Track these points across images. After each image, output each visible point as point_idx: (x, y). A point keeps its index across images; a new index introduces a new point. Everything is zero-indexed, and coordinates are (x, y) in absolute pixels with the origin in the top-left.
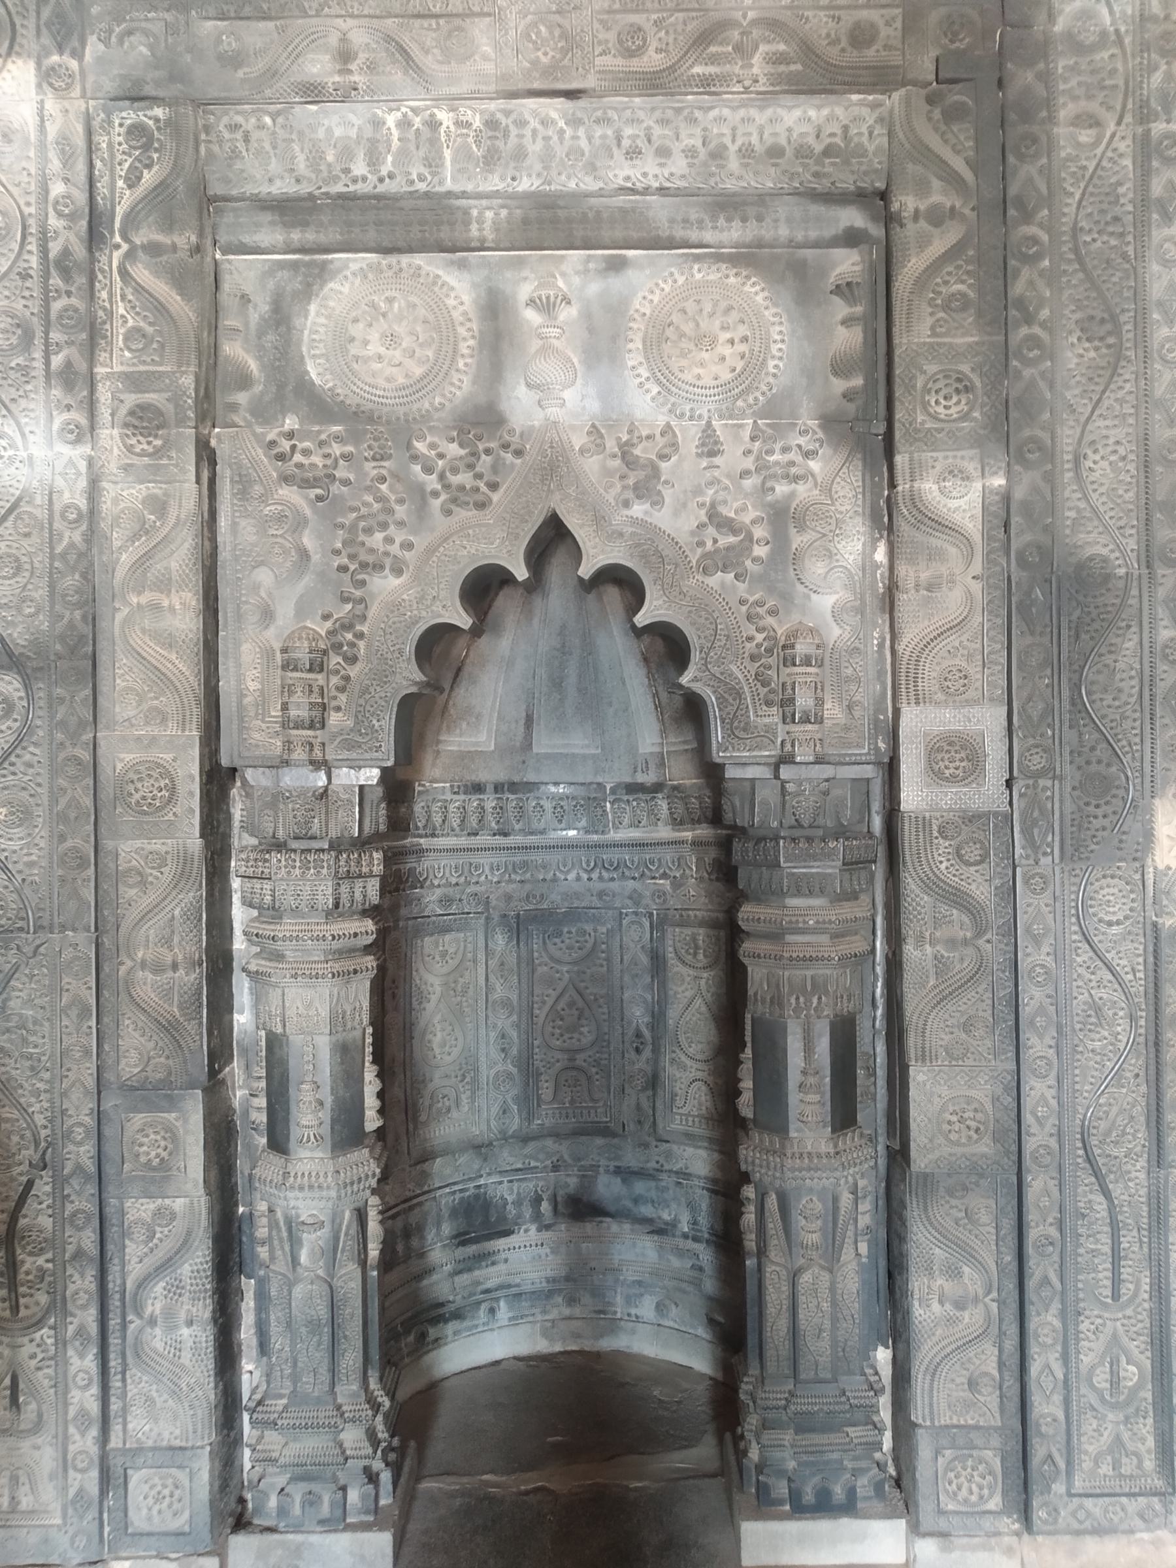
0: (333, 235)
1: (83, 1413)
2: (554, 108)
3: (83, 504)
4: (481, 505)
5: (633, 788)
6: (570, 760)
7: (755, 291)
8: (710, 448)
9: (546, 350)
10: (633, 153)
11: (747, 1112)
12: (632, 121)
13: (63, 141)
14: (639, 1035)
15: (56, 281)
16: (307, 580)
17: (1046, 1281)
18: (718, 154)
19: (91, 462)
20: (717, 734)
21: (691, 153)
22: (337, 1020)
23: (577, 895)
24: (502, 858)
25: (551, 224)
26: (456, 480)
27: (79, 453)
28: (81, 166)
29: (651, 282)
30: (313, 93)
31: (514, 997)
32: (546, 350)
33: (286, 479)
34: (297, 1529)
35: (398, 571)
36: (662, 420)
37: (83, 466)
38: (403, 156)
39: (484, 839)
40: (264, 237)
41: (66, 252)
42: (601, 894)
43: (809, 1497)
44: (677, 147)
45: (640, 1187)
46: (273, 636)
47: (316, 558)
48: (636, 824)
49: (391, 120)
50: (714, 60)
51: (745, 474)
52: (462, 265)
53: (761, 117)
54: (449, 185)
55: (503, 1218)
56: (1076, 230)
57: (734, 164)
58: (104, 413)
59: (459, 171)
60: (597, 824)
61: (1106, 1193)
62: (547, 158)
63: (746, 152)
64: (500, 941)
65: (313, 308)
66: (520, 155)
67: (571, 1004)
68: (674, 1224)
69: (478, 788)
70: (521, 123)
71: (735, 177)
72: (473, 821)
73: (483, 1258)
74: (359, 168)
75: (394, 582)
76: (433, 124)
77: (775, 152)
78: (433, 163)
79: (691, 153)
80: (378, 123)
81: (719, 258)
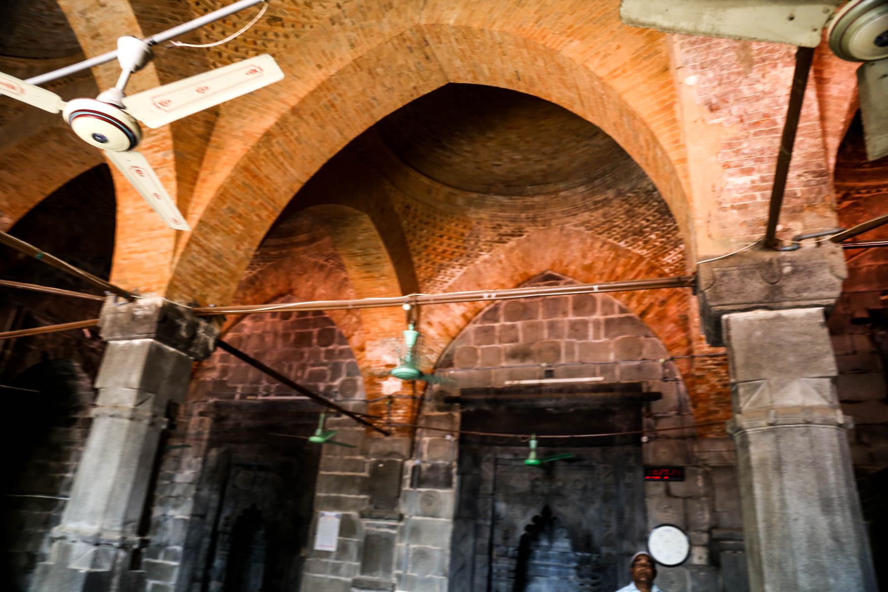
25: (261, 468)
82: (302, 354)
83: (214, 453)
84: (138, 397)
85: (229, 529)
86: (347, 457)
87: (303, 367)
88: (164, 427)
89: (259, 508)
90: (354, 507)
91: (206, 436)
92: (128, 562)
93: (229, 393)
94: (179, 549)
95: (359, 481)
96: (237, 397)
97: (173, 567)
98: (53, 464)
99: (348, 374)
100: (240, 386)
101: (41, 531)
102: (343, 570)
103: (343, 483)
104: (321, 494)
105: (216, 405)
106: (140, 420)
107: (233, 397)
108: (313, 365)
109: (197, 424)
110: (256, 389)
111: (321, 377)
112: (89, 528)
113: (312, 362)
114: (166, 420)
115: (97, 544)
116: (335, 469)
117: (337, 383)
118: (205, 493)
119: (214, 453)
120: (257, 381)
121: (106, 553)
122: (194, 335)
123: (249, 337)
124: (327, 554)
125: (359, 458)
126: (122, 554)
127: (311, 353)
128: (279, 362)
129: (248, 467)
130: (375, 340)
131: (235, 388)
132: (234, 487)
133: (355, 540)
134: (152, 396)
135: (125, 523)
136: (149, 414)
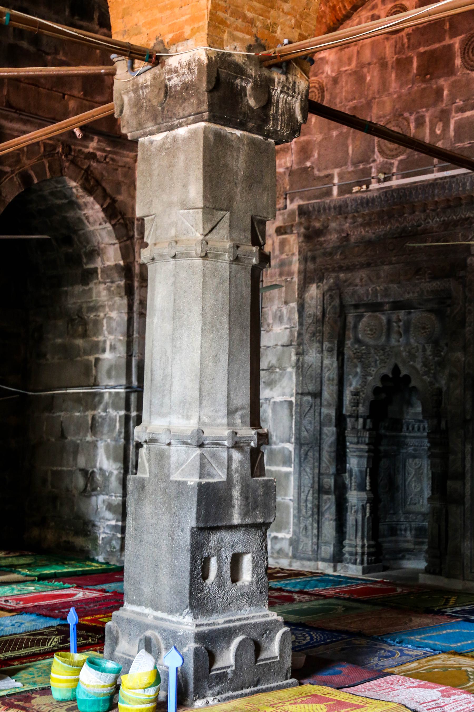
4: (385, 363)
7: (433, 317)
8: (424, 350)
10: (409, 293)
16: (358, 378)
21: (418, 292)
25: (397, 306)
29: (416, 315)
33: (355, 358)
34: (348, 563)
36: (416, 344)
46: (352, 388)
49: (370, 289)
52: (384, 314)
53: (430, 284)
54: (379, 300)
57: (425, 294)
58: (324, 349)
59: (381, 299)
63: (427, 291)
65: (361, 324)
74: (365, 299)
78: (377, 297)
79: (418, 292)
80: (368, 290)
83: (313, 291)
84: (205, 221)
85: (362, 409)
87: (444, 116)
88: (254, 261)
89: (404, 372)
91: (295, 267)
92: (248, 466)
93: (321, 186)
94: (290, 447)
96: (335, 191)
97: (287, 475)
98: (79, 342)
100: (336, 171)
101: (89, 438)
105: (302, 211)
106: (217, 256)
107: (329, 193)
108: (462, 110)
109: (286, 250)
110: (367, 172)
112: (187, 424)
113: (459, 103)
114: (254, 249)
115: (201, 445)
118: (312, 357)
119: (313, 291)
120: (366, 158)
121: (214, 455)
122: (268, 103)
123: (335, 81)
126: (236, 456)
127: (453, 85)
128: (398, 115)
129: (375, 307)
131: (330, 177)
132: (357, 341)
134: (228, 214)
135: (231, 413)
136: (228, 244)
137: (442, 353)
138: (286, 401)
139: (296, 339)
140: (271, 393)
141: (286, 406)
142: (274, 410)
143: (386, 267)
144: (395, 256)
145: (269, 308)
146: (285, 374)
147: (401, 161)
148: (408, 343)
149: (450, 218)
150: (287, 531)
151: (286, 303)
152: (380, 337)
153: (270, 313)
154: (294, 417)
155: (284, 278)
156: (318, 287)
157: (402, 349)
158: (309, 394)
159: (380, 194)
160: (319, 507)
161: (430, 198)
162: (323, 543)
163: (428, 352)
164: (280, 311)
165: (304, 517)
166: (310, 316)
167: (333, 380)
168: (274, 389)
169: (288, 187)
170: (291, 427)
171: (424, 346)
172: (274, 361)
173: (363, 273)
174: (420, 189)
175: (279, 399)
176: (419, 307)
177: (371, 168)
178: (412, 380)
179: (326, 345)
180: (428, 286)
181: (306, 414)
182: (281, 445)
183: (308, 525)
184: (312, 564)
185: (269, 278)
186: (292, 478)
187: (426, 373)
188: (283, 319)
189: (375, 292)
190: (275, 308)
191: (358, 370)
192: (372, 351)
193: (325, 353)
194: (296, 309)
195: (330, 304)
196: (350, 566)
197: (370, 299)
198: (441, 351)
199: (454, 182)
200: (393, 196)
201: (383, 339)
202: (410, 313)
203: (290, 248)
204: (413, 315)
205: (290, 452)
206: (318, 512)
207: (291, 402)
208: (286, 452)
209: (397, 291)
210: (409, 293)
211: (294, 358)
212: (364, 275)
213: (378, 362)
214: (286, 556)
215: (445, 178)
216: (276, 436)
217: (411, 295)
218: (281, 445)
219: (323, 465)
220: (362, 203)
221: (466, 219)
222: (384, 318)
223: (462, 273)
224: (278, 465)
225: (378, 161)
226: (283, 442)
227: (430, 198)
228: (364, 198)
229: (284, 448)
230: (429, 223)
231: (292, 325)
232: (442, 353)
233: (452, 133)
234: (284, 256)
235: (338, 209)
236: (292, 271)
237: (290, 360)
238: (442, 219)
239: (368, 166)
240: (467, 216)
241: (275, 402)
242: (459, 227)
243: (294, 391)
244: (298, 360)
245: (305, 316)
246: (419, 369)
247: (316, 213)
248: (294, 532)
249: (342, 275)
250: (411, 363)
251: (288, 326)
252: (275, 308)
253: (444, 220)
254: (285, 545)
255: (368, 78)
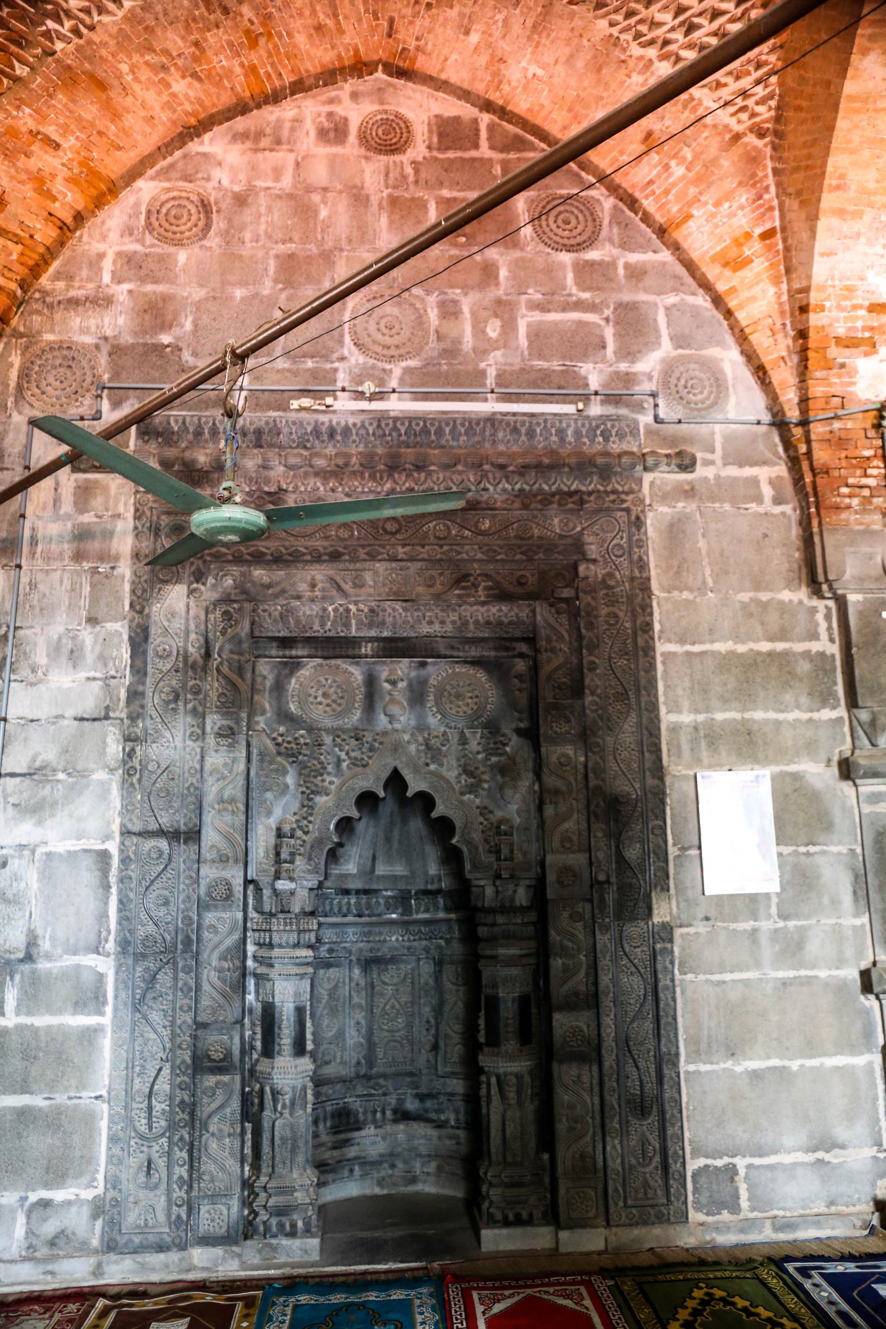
0: (305, 652)
1: (181, 1178)
2: (398, 606)
3: (198, 767)
4: (364, 766)
5: (426, 892)
6: (395, 878)
7: (482, 676)
8: (463, 741)
9: (393, 701)
10: (430, 623)
11: (482, 1040)
12: (430, 610)
13: (197, 617)
14: (428, 1022)
15: (190, 673)
16: (287, 798)
17: (613, 1108)
18: (465, 624)
19: (202, 748)
20: (468, 866)
21: (454, 622)
22: (297, 994)
23: (396, 949)
24: (358, 929)
25: (394, 648)
26: (353, 754)
27: (196, 746)
28: (203, 627)
29: (437, 672)
30: (298, 597)
31: (363, 1002)
32: (393, 701)
33: (279, 753)
34: (274, 1236)
35: (327, 794)
36: (442, 729)
37: (198, 750)
38: (334, 622)
39: (350, 919)
40: (274, 652)
41: (195, 662)
42: (409, 948)
43: (511, 1217)
44: (448, 620)
45: (429, 1104)
47: (292, 787)
48: (427, 911)
49: (330, 609)
50: (463, 588)
51: (478, 753)
52: (357, 664)
53: (483, 609)
54: (354, 633)
55: (357, 1121)
56: (610, 658)
57: (472, 627)
58: (208, 729)
59: (358, 629)
60: (407, 910)
61: (637, 1067)
62: (394, 625)
63: (477, 622)
64: (357, 971)
65: (293, 681)
66: (383, 623)
67: (393, 1007)
68: (447, 1121)
69: (347, 892)
70: (384, 610)
71: (472, 632)
72: (344, 910)
73: (347, 1142)
74: (316, 627)
75: (325, 798)
76: (348, 610)
77: (488, 623)
78: (347, 625)
80: (325, 610)
81: (466, 662)
82: (489, 272)
86: (745, 597)
89: (415, 785)
90: (810, 748)
91: (124, 542)
94: (105, 966)
95: (805, 667)
97: (90, 1035)
99: (679, 341)
102: (813, 947)
103: (752, 675)
104: (676, 715)
111: (588, 344)
113: (536, 296)
116: (712, 634)
117: (649, 364)
124: (752, 903)
125: (786, 595)
127: (517, 266)
130: (858, 215)
133: (833, 849)
137: (508, 749)
138: (86, 851)
139: (122, 703)
140: (40, 830)
141: (87, 862)
142: (47, 874)
143: (380, 566)
144: (404, 546)
145: (37, 630)
146: (87, 786)
147: (407, 371)
148: (421, 727)
149: (536, 486)
150: (84, 1180)
151: (92, 621)
152: (347, 711)
153: (41, 641)
154: (114, 890)
155: (86, 565)
156: (191, 592)
157: (406, 737)
158: (161, 833)
159: (363, 423)
160: (191, 1108)
161: (487, 445)
162: (206, 1196)
163: (474, 745)
164: (74, 638)
165: (142, 1137)
166: (163, 656)
167: (232, 800)
168: (48, 822)
169: (106, 377)
170: (103, 916)
171: (462, 734)
172: (50, 755)
173: (320, 573)
174: (463, 425)
175: (61, 847)
176: (448, 653)
177: (336, 370)
178: (438, 802)
179: (214, 721)
180: (481, 612)
181: (152, 882)
182: (70, 961)
183: (155, 1156)
184: (173, 1256)
185: (40, 562)
186: (106, 1043)
187: (472, 789)
188: (82, 657)
189: (344, 618)
190: (57, 629)
191: (290, 780)
192: (328, 740)
193: (211, 740)
194: (125, 637)
195: (224, 633)
196: (285, 1242)
197: (330, 629)
198: (505, 745)
199: (538, 424)
200: (395, 428)
201: (357, 715)
202: (423, 665)
203: (107, 502)
204: (430, 668)
205: (101, 977)
206: (189, 1118)
207: (104, 856)
208: (86, 976)
209: (398, 619)
210: (430, 623)
211: (115, 748)
212: (319, 577)
213: (345, 765)
214: (83, 1249)
215: (514, 414)
216: (53, 939)
217: (437, 627)
218: (70, 961)
219: (205, 1002)
220: (317, 432)
221: (571, 494)
222: (357, 673)
223: (566, 593)
224: (60, 1012)
225: (353, 361)
226: (75, 953)
227: (487, 445)
228: (323, 423)
229: (78, 967)
230: (485, 489)
231: (113, 673)
232: (508, 749)
233: (523, 342)
234: (88, 518)
235: (251, 436)
236: (113, 552)
237: (103, 752)
238: (518, 487)
239: (328, 366)
240: (573, 488)
241: (49, 855)
242: (555, 506)
243: (116, 827)
244: (131, 754)
245: (151, 653)
246: (453, 781)
247: (190, 437)
248: (113, 1183)
249: (259, 573)
250: (433, 767)
251: (98, 675)
252: (57, 629)
253: (521, 490)
254: (79, 1222)
255: (324, 213)
